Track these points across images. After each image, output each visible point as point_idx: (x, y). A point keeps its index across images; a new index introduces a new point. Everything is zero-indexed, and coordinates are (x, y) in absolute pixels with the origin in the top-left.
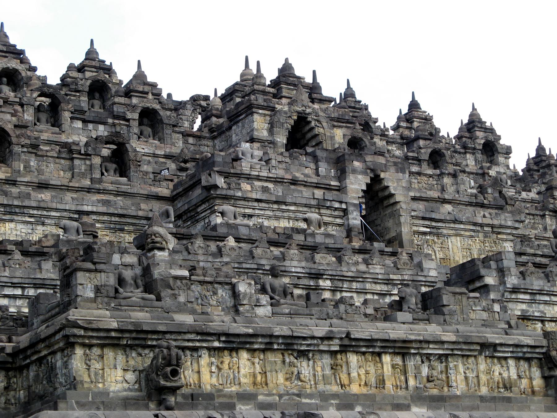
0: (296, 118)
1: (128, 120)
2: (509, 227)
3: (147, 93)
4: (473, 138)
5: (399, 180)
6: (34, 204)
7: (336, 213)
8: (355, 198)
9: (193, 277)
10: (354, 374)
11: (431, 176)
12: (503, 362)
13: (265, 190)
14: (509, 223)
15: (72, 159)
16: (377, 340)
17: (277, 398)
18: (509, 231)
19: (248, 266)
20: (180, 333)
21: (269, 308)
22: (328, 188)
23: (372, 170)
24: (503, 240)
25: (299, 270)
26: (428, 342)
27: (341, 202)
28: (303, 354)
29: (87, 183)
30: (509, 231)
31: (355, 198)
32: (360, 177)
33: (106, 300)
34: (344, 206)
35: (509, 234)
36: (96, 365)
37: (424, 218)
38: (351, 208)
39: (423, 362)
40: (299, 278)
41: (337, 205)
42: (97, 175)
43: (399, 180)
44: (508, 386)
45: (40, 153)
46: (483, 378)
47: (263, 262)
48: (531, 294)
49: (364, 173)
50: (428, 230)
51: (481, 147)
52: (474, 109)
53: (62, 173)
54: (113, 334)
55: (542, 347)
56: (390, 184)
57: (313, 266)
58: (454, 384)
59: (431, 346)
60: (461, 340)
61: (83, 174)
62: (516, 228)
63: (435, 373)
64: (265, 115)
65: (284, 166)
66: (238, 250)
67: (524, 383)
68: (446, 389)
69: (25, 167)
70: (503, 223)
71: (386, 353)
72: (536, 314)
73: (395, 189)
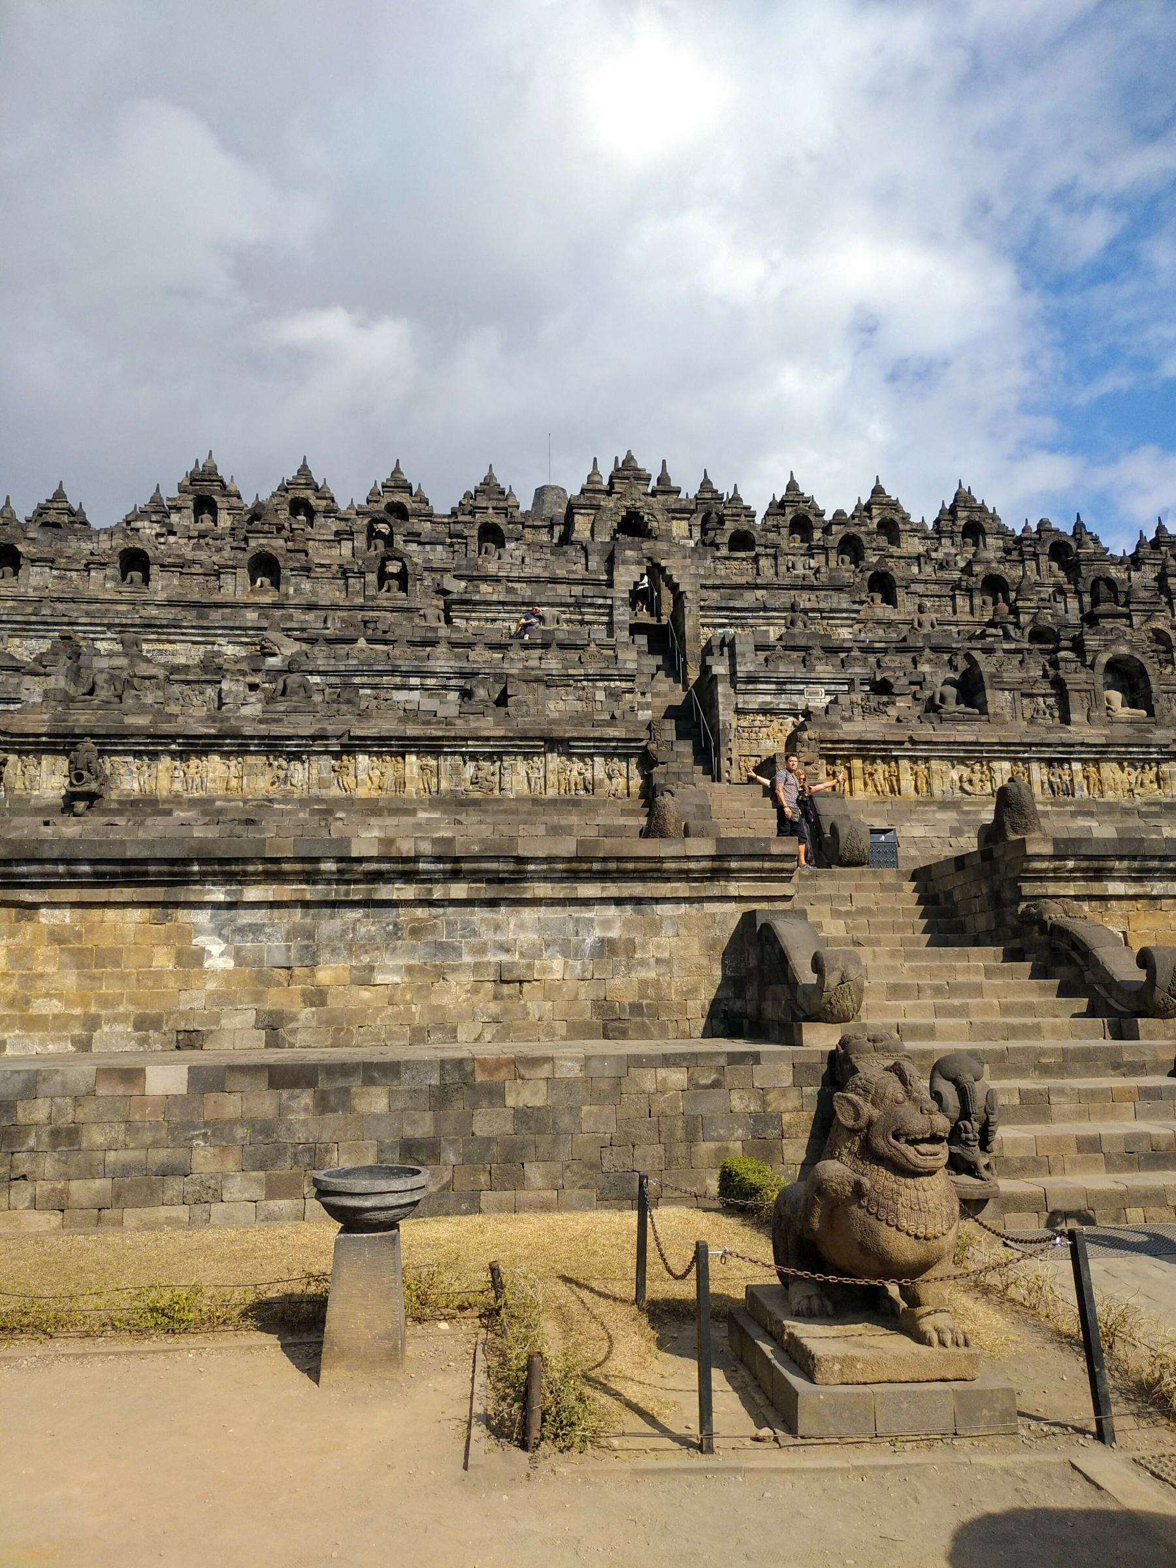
1: (465, 538)
2: (846, 611)
3: (487, 508)
4: (954, 519)
5: (684, 567)
6: (295, 625)
8: (624, 592)
9: (172, 677)
10: (362, 776)
11: (743, 559)
12: (588, 760)
14: (844, 606)
15: (347, 578)
16: (390, 738)
17: (241, 804)
18: (845, 615)
19: (380, 668)
20: (125, 736)
22: (597, 583)
23: (650, 559)
24: (837, 626)
25: (445, 670)
26: (466, 739)
27: (606, 598)
28: (295, 756)
29: (360, 601)
30: (845, 615)
31: (624, 592)
32: (633, 567)
33: (53, 703)
34: (609, 602)
35: (847, 618)
36: (31, 770)
37: (719, 609)
38: (618, 603)
39: (465, 763)
40: (449, 678)
41: (600, 601)
42: (371, 592)
43: (684, 567)
44: (590, 787)
45: (313, 575)
46: (552, 778)
47: (399, 662)
48: (776, 683)
49: (639, 563)
50: (726, 621)
51: (961, 530)
52: (877, 481)
53: (338, 593)
54: (44, 739)
55: (642, 740)
56: (674, 572)
57: (465, 665)
58: (508, 786)
59: (470, 743)
60: (511, 735)
61: (358, 592)
62: (858, 612)
63: (480, 774)
64: (588, 515)
65: (543, 563)
66: (368, 652)
67: (620, 782)
68: (496, 792)
69: (295, 590)
70: (834, 606)
71: (411, 753)
72: (781, 706)
73: (680, 577)
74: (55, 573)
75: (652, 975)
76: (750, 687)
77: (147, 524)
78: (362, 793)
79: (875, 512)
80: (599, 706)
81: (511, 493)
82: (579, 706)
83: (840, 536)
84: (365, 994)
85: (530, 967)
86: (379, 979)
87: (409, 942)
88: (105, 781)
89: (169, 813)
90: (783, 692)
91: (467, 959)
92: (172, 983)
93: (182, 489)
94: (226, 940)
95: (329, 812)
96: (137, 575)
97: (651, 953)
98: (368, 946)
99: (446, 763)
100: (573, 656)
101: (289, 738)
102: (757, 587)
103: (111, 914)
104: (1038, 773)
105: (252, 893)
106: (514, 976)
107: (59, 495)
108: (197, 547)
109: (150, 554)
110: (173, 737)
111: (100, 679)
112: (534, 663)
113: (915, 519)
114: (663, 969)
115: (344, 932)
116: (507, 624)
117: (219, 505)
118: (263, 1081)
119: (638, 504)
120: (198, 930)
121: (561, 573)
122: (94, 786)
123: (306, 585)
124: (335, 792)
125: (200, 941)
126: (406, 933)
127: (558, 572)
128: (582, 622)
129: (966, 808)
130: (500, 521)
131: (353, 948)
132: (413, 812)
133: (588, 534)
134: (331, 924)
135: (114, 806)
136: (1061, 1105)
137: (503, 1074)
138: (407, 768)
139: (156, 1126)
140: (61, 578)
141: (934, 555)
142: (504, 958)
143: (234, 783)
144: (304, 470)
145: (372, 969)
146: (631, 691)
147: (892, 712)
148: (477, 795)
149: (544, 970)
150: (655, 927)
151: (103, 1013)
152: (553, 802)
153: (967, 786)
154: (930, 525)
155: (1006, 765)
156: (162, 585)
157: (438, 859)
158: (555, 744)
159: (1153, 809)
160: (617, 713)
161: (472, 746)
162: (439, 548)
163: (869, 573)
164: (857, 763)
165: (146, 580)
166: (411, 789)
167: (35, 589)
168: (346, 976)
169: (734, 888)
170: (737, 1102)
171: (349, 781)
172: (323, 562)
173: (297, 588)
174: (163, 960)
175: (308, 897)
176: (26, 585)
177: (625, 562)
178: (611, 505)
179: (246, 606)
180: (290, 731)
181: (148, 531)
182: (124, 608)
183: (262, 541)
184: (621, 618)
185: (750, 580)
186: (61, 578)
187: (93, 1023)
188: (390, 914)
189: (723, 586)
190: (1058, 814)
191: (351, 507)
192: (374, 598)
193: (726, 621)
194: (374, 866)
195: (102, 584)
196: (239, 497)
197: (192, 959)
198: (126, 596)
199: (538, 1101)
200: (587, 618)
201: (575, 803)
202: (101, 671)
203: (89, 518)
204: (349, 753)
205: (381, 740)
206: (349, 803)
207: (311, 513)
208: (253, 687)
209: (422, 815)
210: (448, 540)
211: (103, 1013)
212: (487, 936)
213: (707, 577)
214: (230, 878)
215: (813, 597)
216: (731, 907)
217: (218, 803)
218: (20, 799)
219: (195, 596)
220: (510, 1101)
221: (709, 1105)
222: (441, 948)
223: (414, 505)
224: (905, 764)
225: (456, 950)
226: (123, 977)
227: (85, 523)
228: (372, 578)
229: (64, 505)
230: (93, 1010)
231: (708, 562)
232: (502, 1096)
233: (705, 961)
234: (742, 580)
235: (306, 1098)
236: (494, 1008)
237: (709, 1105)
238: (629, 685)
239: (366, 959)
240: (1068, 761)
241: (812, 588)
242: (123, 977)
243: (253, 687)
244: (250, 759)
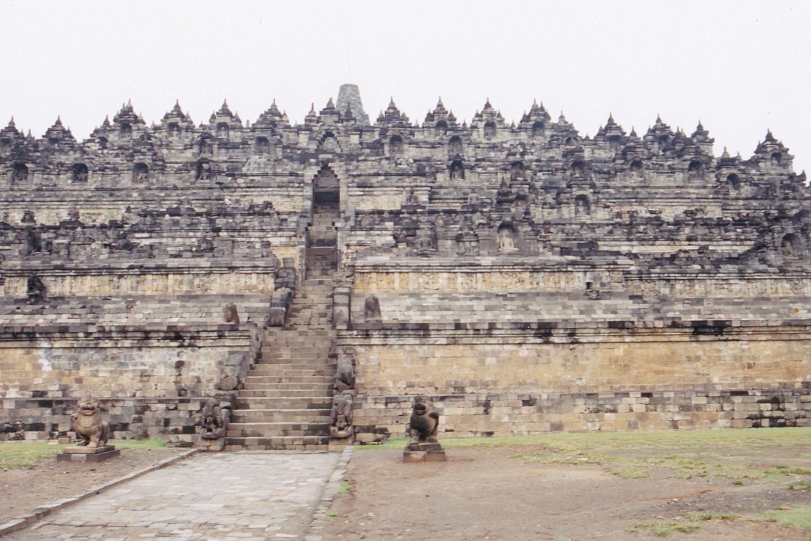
0: (324, 133)
5: (340, 167)
7: (299, 189)
14: (424, 184)
21: (107, 255)
28: (121, 276)
32: (314, 167)
34: (302, 185)
42: (193, 180)
43: (340, 167)
46: (233, 285)
49: (317, 164)
50: (362, 193)
70: (418, 184)
73: (338, 171)
74: (45, 176)
75: (196, 374)
76: (353, 233)
77: (92, 144)
78: (149, 293)
79: (484, 118)
80: (257, 251)
81: (285, 114)
82: (248, 251)
83: (450, 137)
84: (96, 380)
85: (153, 371)
86: (100, 374)
87: (110, 362)
88: (43, 288)
89: (68, 303)
90: (370, 235)
91: (131, 368)
92: (32, 375)
93: (115, 120)
94: (49, 361)
95: (134, 302)
96: (83, 176)
97: (196, 367)
98: (96, 363)
99: (186, 278)
100: (266, 219)
101: (118, 269)
102: (379, 175)
103: (12, 351)
104: (460, 279)
105: (57, 345)
106: (147, 374)
107: (58, 123)
108: (117, 155)
109: (88, 165)
110: (70, 269)
111: (43, 244)
112: (246, 224)
113: (508, 122)
114: (200, 372)
115: (88, 359)
116: (251, 198)
117: (133, 128)
118: (37, 405)
119: (331, 128)
120: (40, 357)
121: (279, 170)
122: (37, 292)
123: (161, 178)
124: (140, 293)
125: (40, 361)
126: (109, 359)
127: (277, 170)
128: (289, 196)
129: (423, 297)
130: (267, 135)
131: (91, 364)
132: (168, 302)
133: (305, 144)
134: (84, 356)
135: (47, 300)
136: (276, 416)
137: (109, 404)
138: (169, 281)
139: (6, 418)
140: (47, 179)
141: (505, 145)
142: (143, 368)
143: (97, 289)
144: (177, 107)
145: (98, 371)
146: (295, 236)
147: (395, 250)
148: (199, 293)
149: (157, 373)
150: (198, 357)
151: (10, 384)
152: (232, 296)
153: (426, 286)
154: (517, 126)
155: (446, 275)
156: (93, 181)
157: (118, 332)
158: (232, 268)
159: (514, 296)
160: (265, 254)
161: (196, 271)
162: (237, 150)
163: (452, 162)
164: (374, 275)
165: (86, 179)
166: (170, 290)
167: (36, 185)
168: (89, 373)
169: (228, 342)
170: (182, 414)
172: (178, 161)
173: (157, 179)
174: (28, 367)
175: (75, 346)
176: (32, 184)
177: (310, 164)
178: (317, 129)
179: (133, 189)
180: (117, 266)
181: (94, 148)
183: (142, 157)
184: (308, 194)
185: (375, 171)
186: (47, 179)
187: (6, 388)
188: (103, 353)
189: (360, 175)
190: (464, 299)
191: (201, 126)
192: (194, 183)
193: (362, 193)
194: (96, 335)
195: (65, 181)
196: (144, 123)
197: (39, 367)
199: (119, 413)
200: (291, 193)
201: (242, 296)
202: (44, 240)
203: (73, 134)
204: (144, 275)
205: (158, 268)
206: (143, 298)
207: (179, 129)
208: (106, 245)
209: (173, 303)
210: (241, 146)
211: (10, 384)
212: (138, 360)
213: (353, 171)
214: (50, 339)
215: (407, 180)
216: (227, 349)
217: (89, 298)
218: (11, 297)
219: (109, 186)
220: (110, 413)
221: (172, 415)
222: (122, 364)
223: (232, 124)
224: (397, 275)
225: (127, 365)
226: (16, 373)
227: (72, 137)
228: (193, 173)
229: (61, 129)
230: (7, 384)
231: (355, 163)
232: (108, 411)
233: (216, 369)
234: (372, 172)
235: (48, 411)
236: (140, 385)
237: (172, 415)
238: (293, 233)
239: (96, 368)
240: (476, 273)
241: (409, 175)
242: (16, 373)
243: (106, 245)
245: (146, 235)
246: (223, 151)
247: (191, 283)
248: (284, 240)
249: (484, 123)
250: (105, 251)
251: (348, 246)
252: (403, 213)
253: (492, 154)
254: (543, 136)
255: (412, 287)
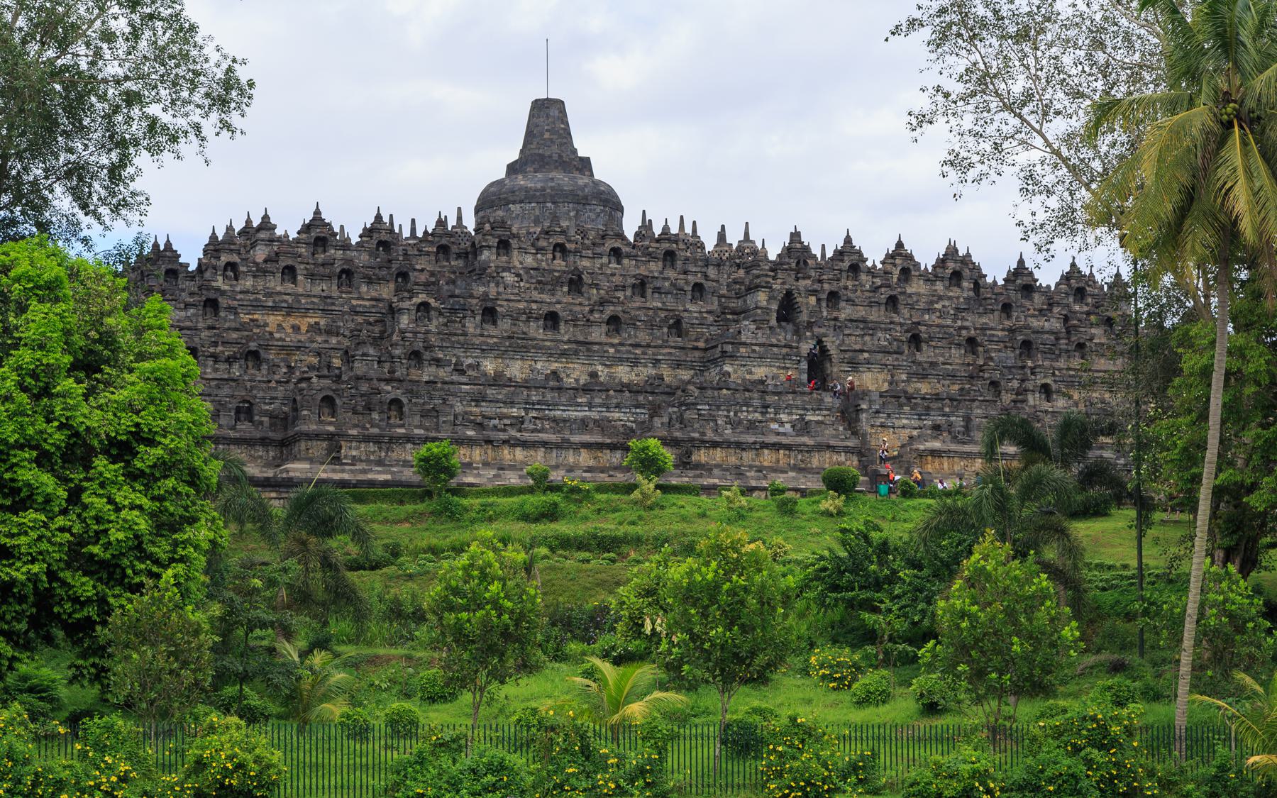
13: (754, 351)
49: (812, 339)
77: (508, 274)
78: (766, 464)
99: (792, 454)
124: (757, 463)
128: (785, 368)
147: (941, 438)
156: (566, 332)
162: (670, 296)
164: (930, 458)
171: (762, 459)
182: (548, 344)
198: (550, 337)
200: (788, 365)
244: (730, 450)
245: (707, 407)
246: (656, 295)
247: (796, 457)
248: (820, 418)
249: (899, 268)
250: (729, 426)
251: (872, 426)
252: (916, 398)
253: (927, 317)
254: (959, 286)
255: (957, 468)
